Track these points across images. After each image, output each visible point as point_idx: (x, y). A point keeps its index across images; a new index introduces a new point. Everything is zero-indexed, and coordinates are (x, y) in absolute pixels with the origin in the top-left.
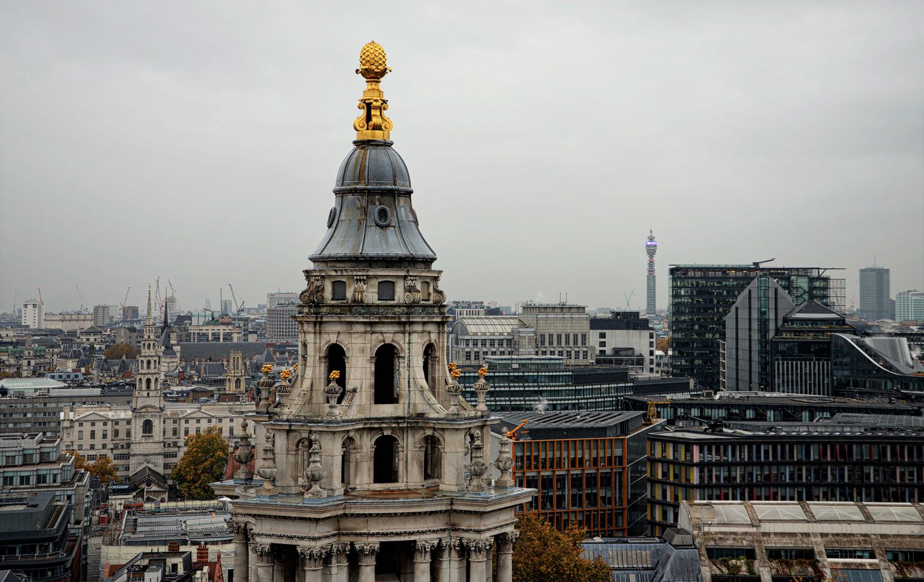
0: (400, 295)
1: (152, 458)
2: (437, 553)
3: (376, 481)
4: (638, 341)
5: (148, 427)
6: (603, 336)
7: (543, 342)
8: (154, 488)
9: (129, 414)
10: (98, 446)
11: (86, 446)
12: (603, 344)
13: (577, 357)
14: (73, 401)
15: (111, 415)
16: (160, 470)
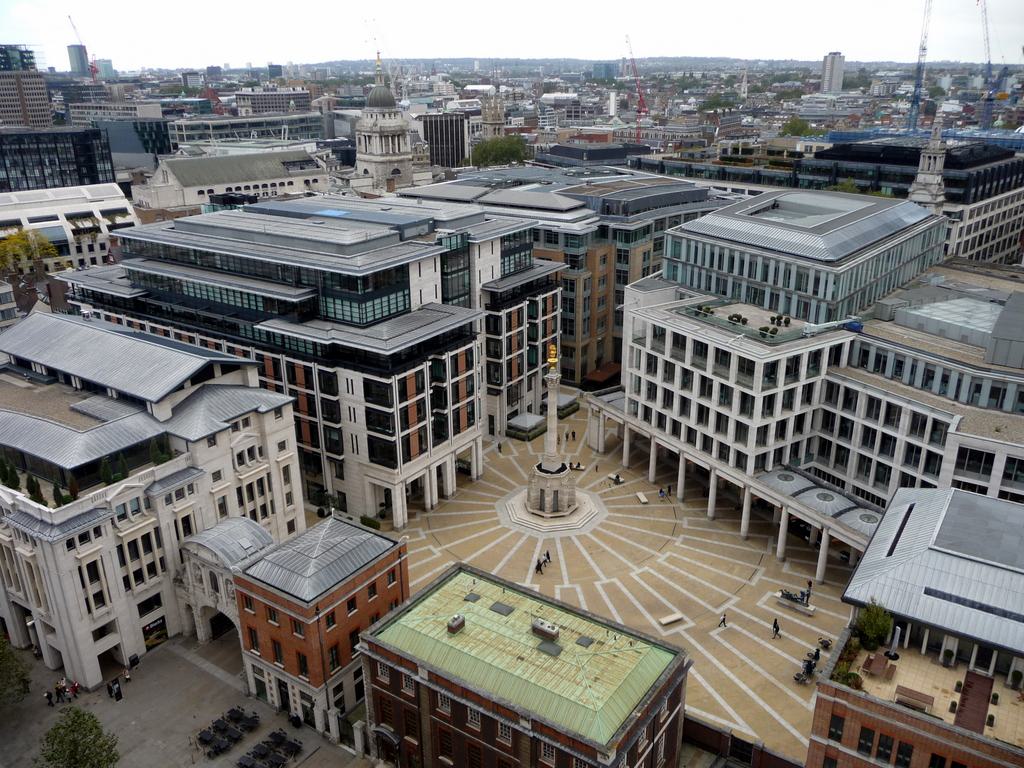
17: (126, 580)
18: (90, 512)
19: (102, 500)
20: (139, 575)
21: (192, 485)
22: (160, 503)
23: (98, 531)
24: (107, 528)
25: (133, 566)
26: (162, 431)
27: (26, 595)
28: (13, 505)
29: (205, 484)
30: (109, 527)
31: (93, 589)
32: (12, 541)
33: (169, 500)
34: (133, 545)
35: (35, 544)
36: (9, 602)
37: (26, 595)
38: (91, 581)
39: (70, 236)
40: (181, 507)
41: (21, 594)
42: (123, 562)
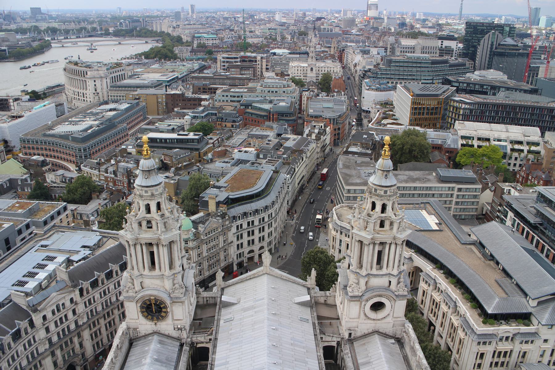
0: (388, 193)
1: (313, 78)
2: (391, 244)
3: (380, 227)
4: (453, 44)
5: (312, 69)
6: (442, 42)
7: (424, 49)
8: (313, 87)
9: (307, 65)
10: (299, 73)
11: (296, 73)
12: (442, 44)
13: (433, 53)
14: (293, 60)
15: (302, 65)
16: (315, 81)
17: (492, 363)
18: (490, 334)
19: (496, 332)
20: (497, 364)
21: (533, 341)
22: (517, 342)
23: (490, 343)
24: (494, 343)
25: (496, 360)
26: (530, 311)
27: (454, 345)
28: (464, 315)
29: (539, 342)
30: (495, 343)
31: (479, 361)
32: (458, 327)
33: (521, 343)
34: (500, 353)
35: (466, 334)
36: (446, 342)
37: (454, 345)
38: (480, 358)
39: (509, 151)
40: (525, 347)
41: (452, 344)
42: (493, 357)
